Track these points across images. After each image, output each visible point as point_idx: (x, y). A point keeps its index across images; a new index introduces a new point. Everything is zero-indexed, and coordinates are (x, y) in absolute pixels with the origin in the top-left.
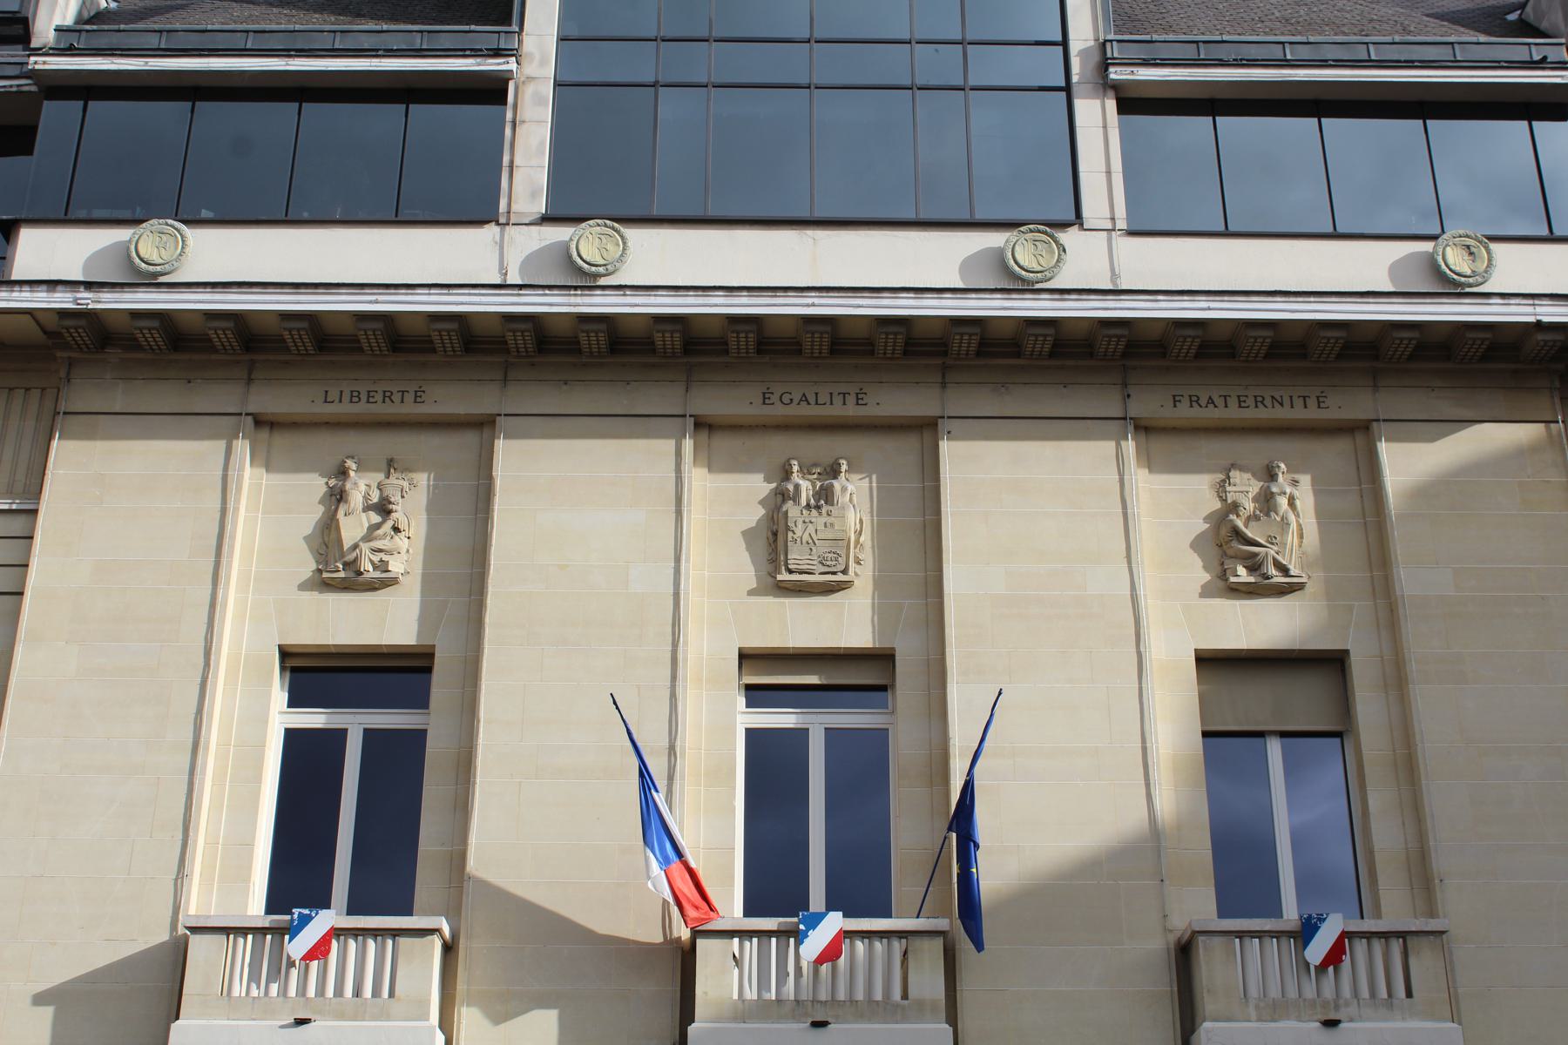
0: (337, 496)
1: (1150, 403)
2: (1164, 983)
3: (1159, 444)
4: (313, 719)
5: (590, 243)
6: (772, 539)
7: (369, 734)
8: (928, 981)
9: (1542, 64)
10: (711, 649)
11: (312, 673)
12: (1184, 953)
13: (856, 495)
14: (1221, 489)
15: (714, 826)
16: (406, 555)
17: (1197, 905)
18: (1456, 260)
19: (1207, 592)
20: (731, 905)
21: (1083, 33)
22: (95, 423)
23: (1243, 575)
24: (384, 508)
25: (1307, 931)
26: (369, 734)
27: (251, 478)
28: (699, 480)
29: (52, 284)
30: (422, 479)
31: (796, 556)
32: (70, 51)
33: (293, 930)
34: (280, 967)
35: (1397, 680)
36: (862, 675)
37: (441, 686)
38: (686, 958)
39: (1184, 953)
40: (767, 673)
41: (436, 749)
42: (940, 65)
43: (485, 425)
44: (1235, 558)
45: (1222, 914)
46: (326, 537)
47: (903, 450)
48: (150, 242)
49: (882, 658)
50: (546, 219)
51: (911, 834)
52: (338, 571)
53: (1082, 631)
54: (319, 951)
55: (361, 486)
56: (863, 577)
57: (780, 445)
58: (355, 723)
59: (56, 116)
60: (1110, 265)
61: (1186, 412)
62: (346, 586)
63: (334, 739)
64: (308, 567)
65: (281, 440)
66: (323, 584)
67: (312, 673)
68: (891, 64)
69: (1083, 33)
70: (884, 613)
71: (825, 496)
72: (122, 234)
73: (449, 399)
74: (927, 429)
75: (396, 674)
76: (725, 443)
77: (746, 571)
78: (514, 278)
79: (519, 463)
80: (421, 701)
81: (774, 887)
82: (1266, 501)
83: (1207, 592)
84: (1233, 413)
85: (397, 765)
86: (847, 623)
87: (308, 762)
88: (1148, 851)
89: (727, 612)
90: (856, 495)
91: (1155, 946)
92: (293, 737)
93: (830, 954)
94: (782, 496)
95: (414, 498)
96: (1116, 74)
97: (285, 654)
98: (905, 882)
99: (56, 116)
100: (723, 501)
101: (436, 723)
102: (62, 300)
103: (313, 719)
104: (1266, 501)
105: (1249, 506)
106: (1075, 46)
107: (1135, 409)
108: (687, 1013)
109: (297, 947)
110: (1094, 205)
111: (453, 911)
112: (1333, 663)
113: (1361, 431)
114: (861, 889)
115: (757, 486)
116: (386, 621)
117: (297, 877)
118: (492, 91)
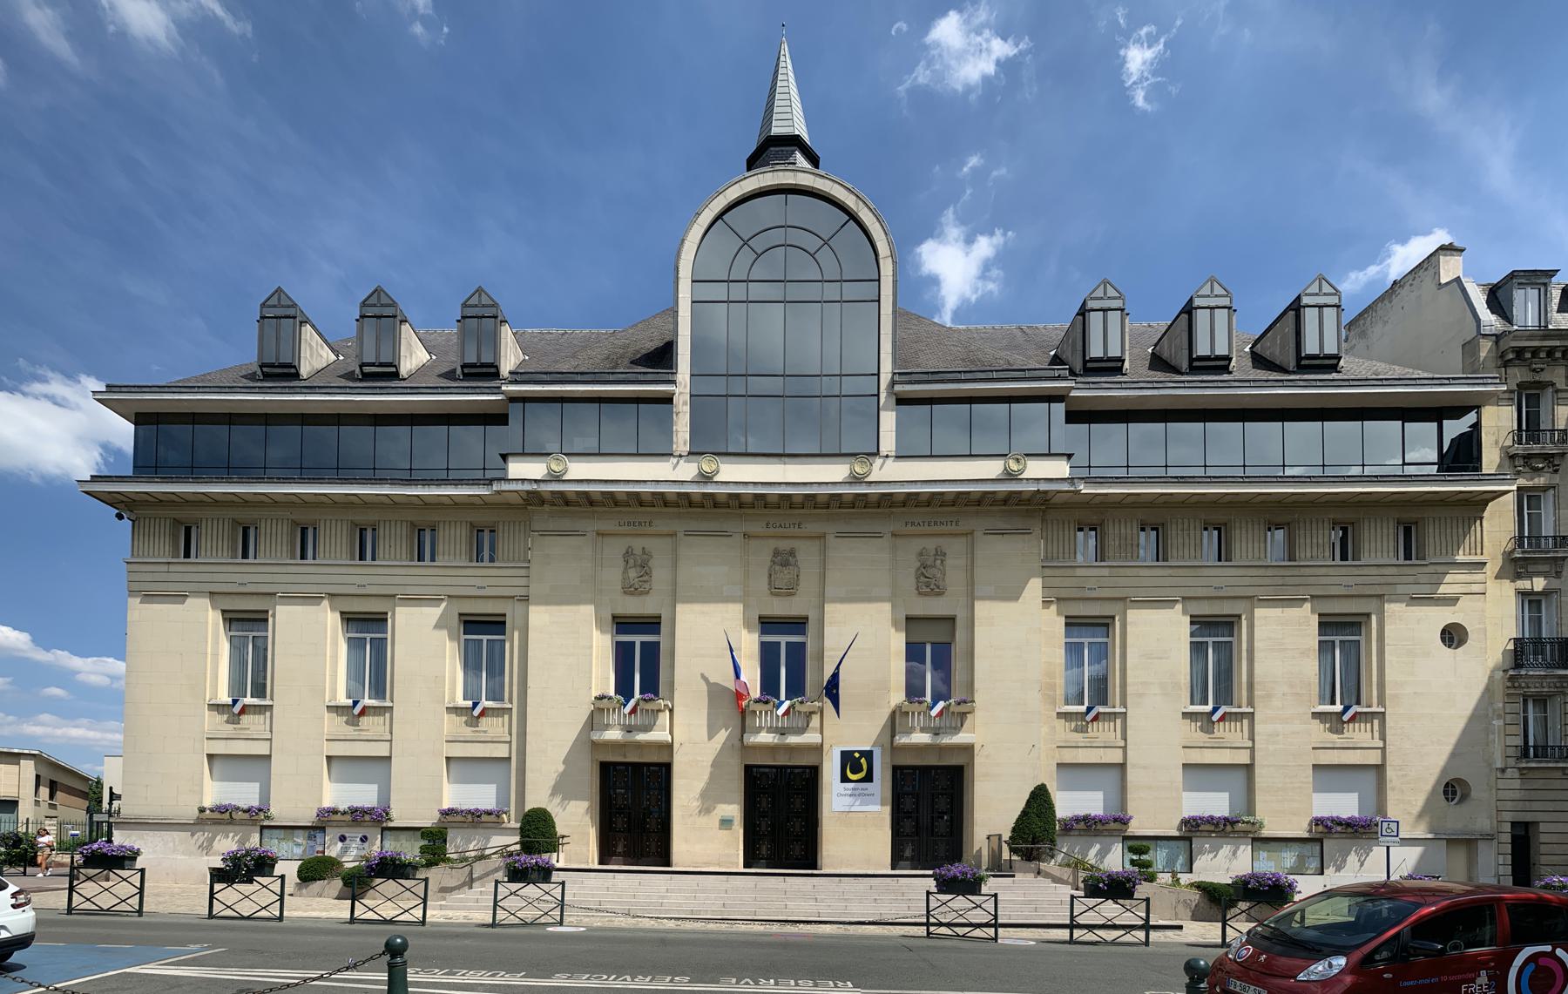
9: (1059, 378)
18: (1014, 466)
29: (523, 480)
32: (516, 382)
42: (831, 386)
59: (515, 411)
62: (632, 594)
68: (814, 386)
69: (885, 378)
85: (652, 653)
97: (614, 617)
99: (515, 411)
101: (662, 639)
102: (527, 487)
110: (884, 450)
117: (624, 687)
118: (668, 400)
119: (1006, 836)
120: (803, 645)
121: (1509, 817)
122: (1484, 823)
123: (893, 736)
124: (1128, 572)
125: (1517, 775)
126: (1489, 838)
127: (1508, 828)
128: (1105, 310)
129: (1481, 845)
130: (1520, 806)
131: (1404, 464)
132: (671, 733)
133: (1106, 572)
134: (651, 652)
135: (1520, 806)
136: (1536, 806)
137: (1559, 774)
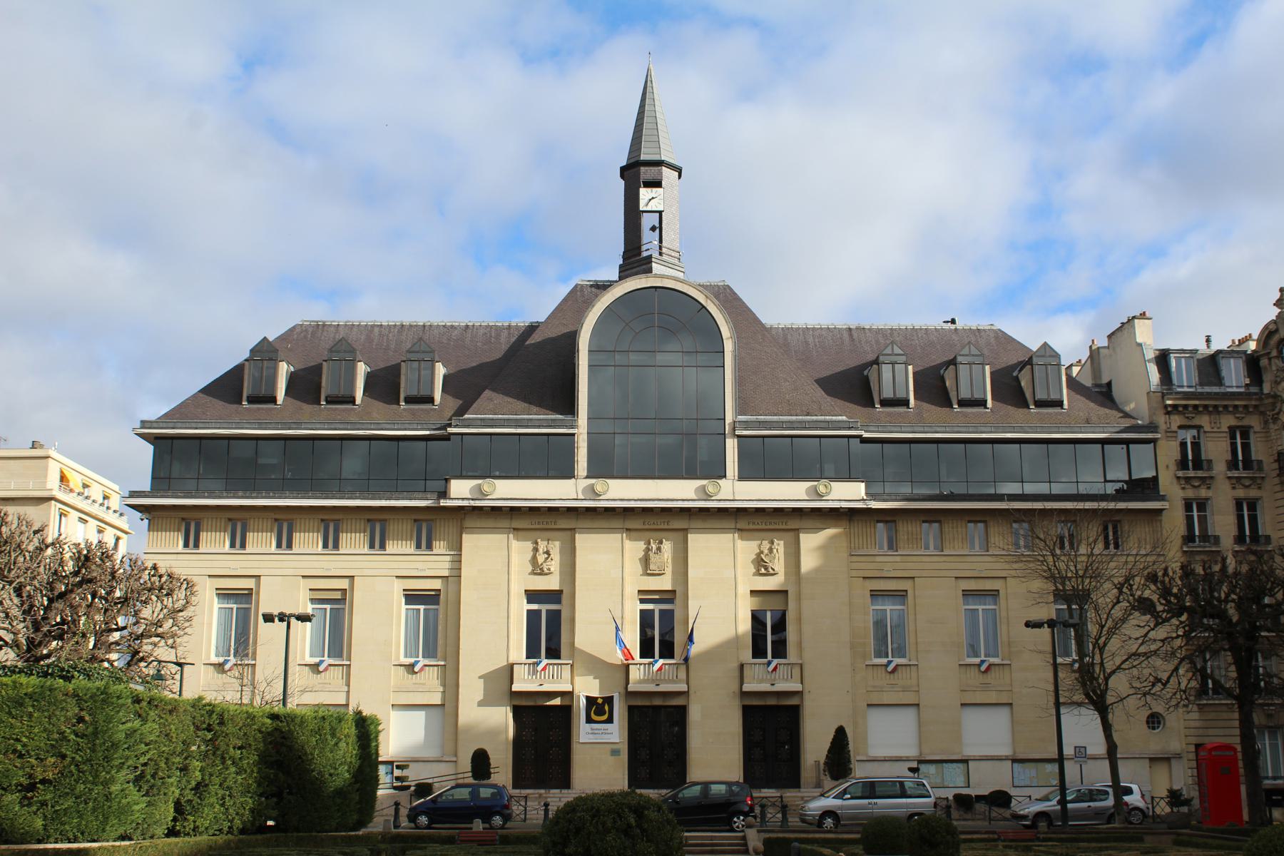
0: (536, 550)
1: (742, 524)
2: (737, 673)
3: (745, 534)
4: (535, 607)
5: (599, 484)
6: (646, 561)
7: (548, 611)
8: (682, 675)
10: (631, 590)
11: (532, 596)
12: (742, 666)
13: (667, 546)
14: (760, 546)
15: (633, 639)
16: (555, 565)
17: (747, 654)
19: (754, 575)
20: (636, 653)
21: (729, 418)
22: (473, 530)
23: (763, 571)
24: (548, 553)
25: (769, 663)
26: (548, 611)
27: (515, 544)
28: (628, 544)
30: (557, 544)
31: (652, 567)
33: (538, 664)
34: (535, 672)
35: (799, 598)
36: (667, 597)
37: (565, 598)
38: (627, 666)
39: (742, 666)
40: (645, 596)
41: (564, 615)
43: (573, 530)
44: (761, 566)
45: (754, 657)
46: (534, 560)
47: (679, 535)
48: (486, 484)
49: (673, 592)
50: (587, 477)
51: (679, 638)
52: (538, 570)
53: (722, 589)
54: (544, 669)
55: (542, 546)
56: (669, 571)
57: (648, 534)
58: (544, 608)
60: (735, 490)
61: (751, 527)
63: (538, 612)
64: (530, 568)
65: (521, 533)
66: (533, 573)
67: (532, 596)
70: (674, 580)
71: (659, 549)
72: (480, 481)
73: (563, 523)
74: (685, 531)
75: (553, 596)
76: (634, 534)
77: (640, 570)
78: (581, 497)
79: (582, 540)
80: (559, 602)
81: (646, 650)
82: (771, 550)
83: (754, 575)
84: (764, 527)
86: (665, 583)
87: (533, 617)
88: (737, 639)
89: (635, 581)
90: (667, 546)
91: (736, 665)
92: (528, 611)
93: (660, 669)
94: (648, 550)
95: (555, 548)
96: (737, 433)
98: (677, 650)
100: (635, 548)
101: (564, 608)
103: (535, 607)
104: (771, 550)
105: (766, 552)
106: (727, 422)
107: (739, 526)
108: (627, 682)
109: (540, 668)
111: (572, 657)
112: (786, 592)
113: (797, 531)
114: (667, 651)
115: (641, 545)
116: (551, 583)
119: (822, 761)
120: (672, 611)
121: (1194, 740)
122: (1175, 745)
123: (742, 683)
124: (914, 559)
125: (1195, 708)
126: (1178, 756)
127: (1192, 748)
128: (893, 364)
129: (1173, 762)
130: (1201, 732)
131: (1106, 481)
132: (572, 683)
133: (898, 559)
134: (554, 618)
135: (1201, 732)
136: (1211, 732)
137: (1224, 708)
